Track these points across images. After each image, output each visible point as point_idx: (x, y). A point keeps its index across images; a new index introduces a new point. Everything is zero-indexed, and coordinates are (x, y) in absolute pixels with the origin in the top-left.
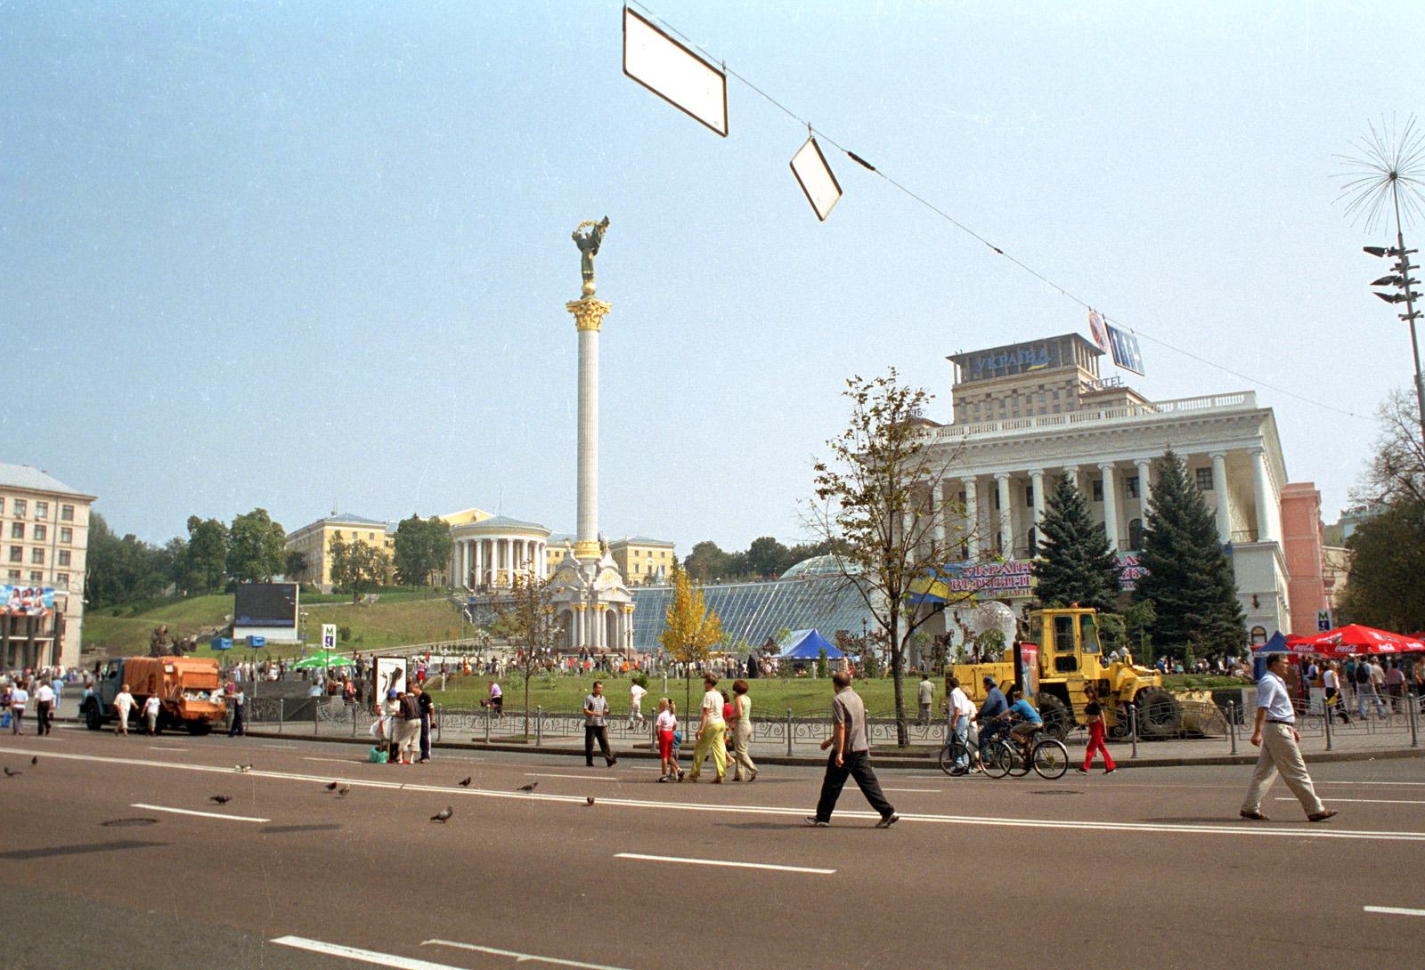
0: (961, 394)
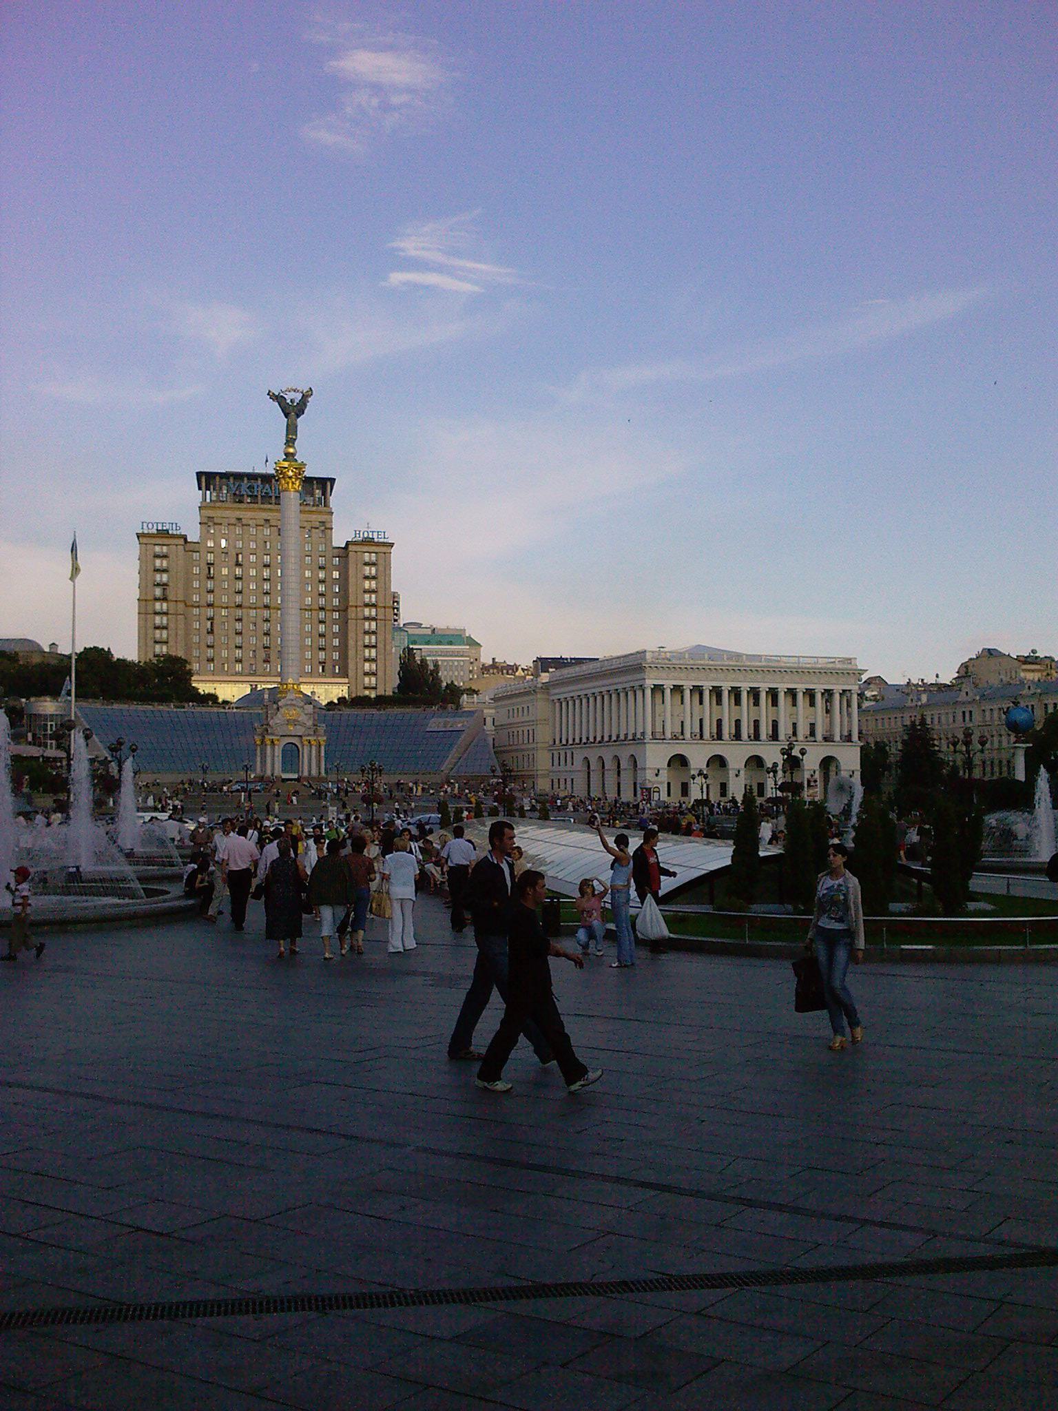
0: (210, 513)
